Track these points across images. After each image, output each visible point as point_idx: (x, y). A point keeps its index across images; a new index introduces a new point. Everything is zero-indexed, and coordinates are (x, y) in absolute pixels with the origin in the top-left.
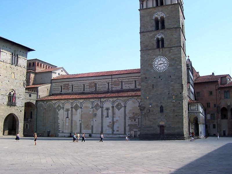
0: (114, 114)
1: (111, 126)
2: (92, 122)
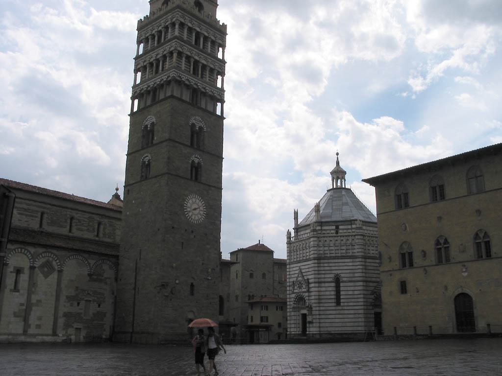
0: (32, 284)
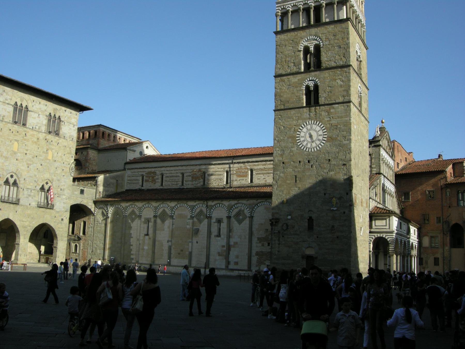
0: (230, 230)
1: (225, 254)
2: (190, 244)
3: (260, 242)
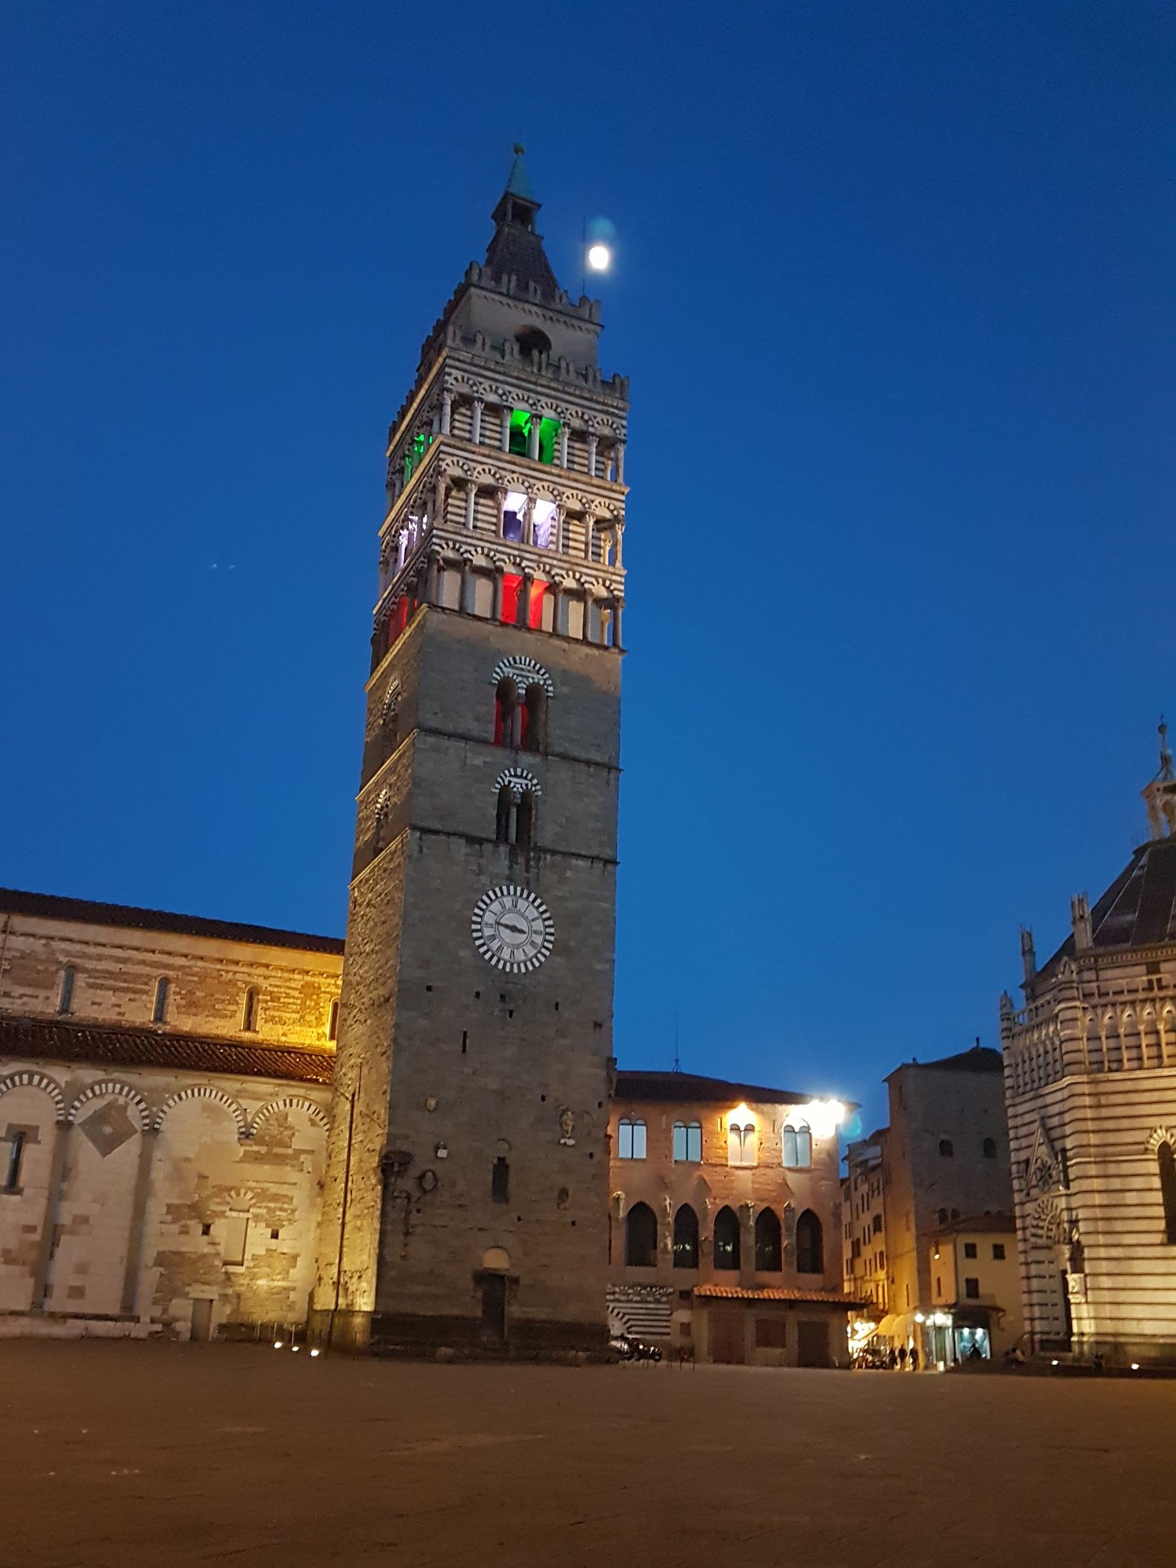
0: (63, 1170)
1: (33, 1256)
3: (174, 1221)
